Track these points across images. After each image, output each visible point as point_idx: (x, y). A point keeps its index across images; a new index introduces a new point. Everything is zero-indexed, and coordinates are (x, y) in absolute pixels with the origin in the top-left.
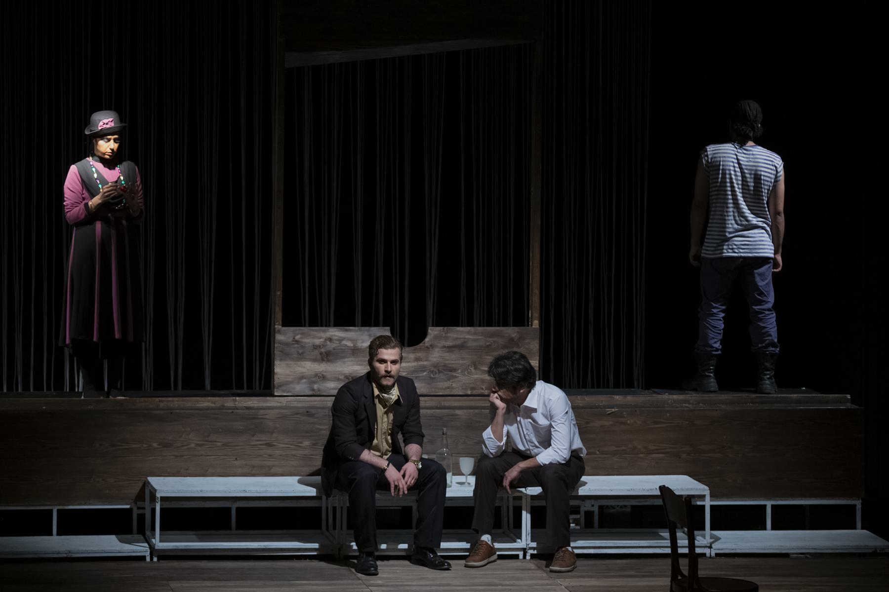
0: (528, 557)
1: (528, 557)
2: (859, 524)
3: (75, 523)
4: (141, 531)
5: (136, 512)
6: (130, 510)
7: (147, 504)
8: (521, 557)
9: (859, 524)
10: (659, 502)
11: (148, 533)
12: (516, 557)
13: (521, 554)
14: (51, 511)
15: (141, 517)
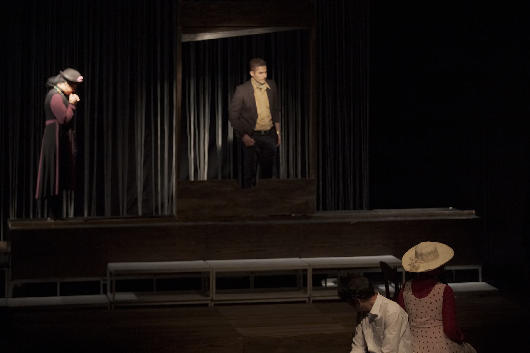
0: (311, 302)
1: (311, 302)
2: (481, 279)
3: (69, 289)
4: (105, 293)
5: (102, 283)
6: (99, 282)
7: (108, 278)
8: (307, 301)
9: (481, 279)
10: (380, 270)
11: (109, 294)
12: (304, 302)
13: (307, 300)
14: (56, 283)
15: (105, 286)
